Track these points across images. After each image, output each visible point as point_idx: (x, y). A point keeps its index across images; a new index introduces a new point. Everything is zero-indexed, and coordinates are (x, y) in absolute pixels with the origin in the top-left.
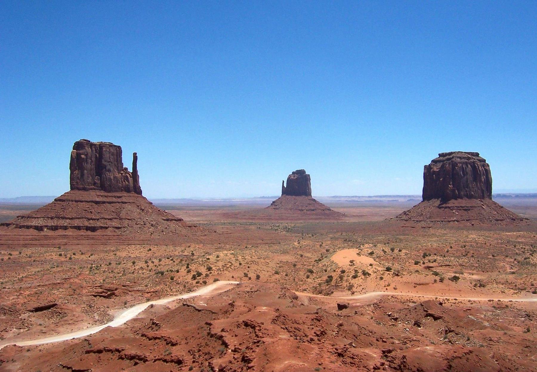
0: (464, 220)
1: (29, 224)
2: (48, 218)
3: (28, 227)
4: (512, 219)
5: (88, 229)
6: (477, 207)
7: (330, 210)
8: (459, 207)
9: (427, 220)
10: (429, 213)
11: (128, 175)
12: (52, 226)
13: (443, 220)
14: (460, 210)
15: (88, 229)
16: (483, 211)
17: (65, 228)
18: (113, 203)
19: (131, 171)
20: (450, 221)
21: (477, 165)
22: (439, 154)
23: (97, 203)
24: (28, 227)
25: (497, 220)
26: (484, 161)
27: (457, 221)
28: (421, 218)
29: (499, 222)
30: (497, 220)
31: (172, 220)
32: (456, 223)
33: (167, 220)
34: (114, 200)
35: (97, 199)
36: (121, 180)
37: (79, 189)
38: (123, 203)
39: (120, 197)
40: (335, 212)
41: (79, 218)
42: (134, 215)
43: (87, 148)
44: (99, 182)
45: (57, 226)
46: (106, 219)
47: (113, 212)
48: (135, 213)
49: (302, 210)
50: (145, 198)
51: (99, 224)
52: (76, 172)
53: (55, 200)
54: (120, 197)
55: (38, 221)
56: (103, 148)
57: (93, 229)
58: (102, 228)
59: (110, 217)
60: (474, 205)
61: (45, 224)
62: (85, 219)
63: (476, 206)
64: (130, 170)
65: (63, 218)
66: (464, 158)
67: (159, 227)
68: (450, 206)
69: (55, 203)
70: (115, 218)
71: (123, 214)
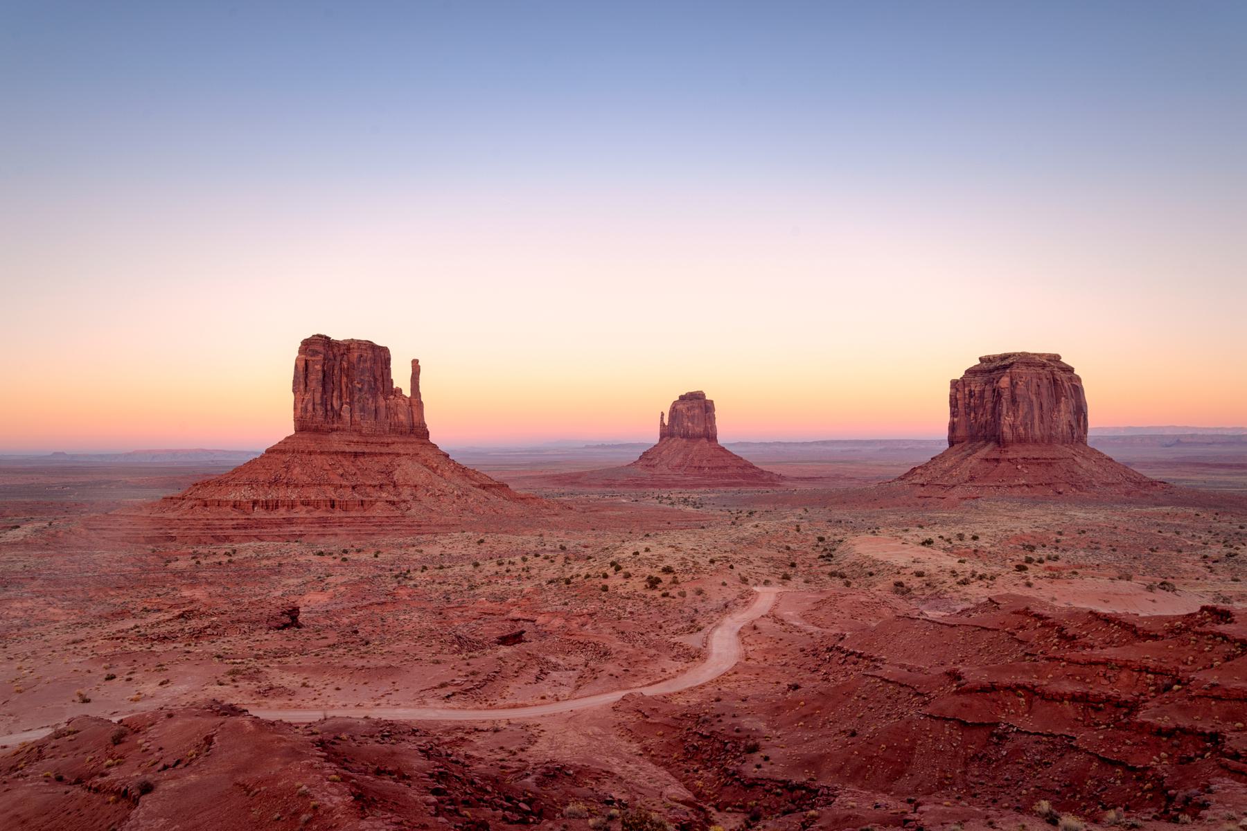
0: (1042, 484)
4: (1135, 483)
6: (1060, 459)
13: (998, 484)
16: (1076, 468)
20: (1015, 486)
25: (1107, 484)
26: (1070, 370)
27: (1027, 486)
28: (955, 481)
30: (1107, 484)
31: (491, 486)
32: (1027, 489)
33: (484, 487)
53: (269, 451)
59: (374, 483)
60: (1057, 454)
68: (1010, 457)
69: (268, 457)
70: (386, 485)
71: (398, 476)
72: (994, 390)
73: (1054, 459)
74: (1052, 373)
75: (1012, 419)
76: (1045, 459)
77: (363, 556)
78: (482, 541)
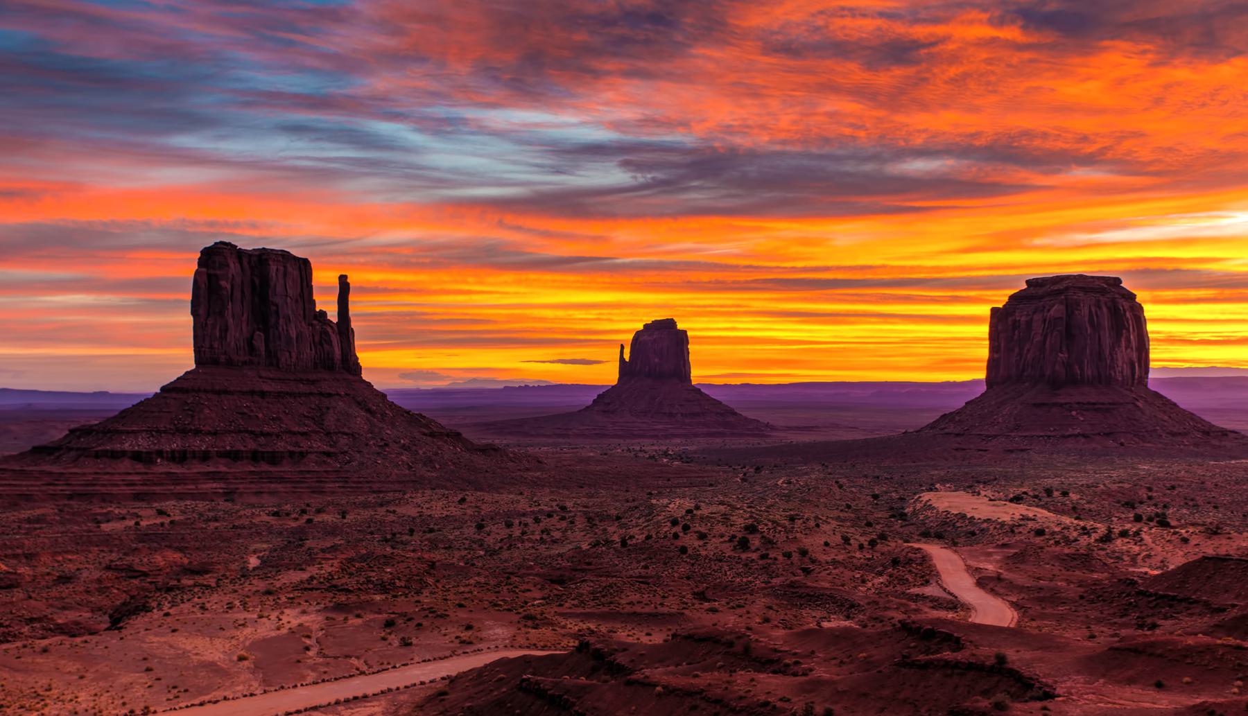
1: (118, 447)
2: (158, 431)
3: (116, 455)
5: (255, 457)
6: (1121, 404)
7: (735, 414)
8: (1084, 404)
9: (1013, 434)
10: (1012, 420)
11: (329, 330)
12: (173, 451)
13: (1049, 433)
14: (1086, 410)
15: (255, 457)
17: (205, 457)
18: (300, 395)
19: (335, 320)
21: (1123, 307)
22: (1027, 282)
23: (263, 394)
24: (116, 455)
25: (1173, 434)
27: (1084, 436)
29: (1179, 439)
30: (1173, 434)
32: (1083, 440)
33: (432, 435)
34: (303, 388)
35: (266, 388)
36: (314, 340)
37: (215, 362)
38: (321, 394)
39: (313, 382)
40: (746, 418)
41: (230, 432)
42: (356, 423)
43: (232, 265)
44: (260, 344)
45: (185, 452)
46: (294, 433)
47: (305, 416)
48: (359, 420)
49: (671, 415)
50: (369, 385)
51: (281, 446)
52: (210, 322)
54: (313, 382)
55: (136, 439)
56: (271, 263)
57: (274, 458)
58: (292, 454)
59: (301, 430)
61: (157, 447)
62: (246, 435)
63: (1122, 401)
64: (333, 316)
65: (197, 432)
66: (1092, 290)
67: (421, 452)
68: (1063, 401)
71: (330, 421)
72: (1045, 321)
73: (1113, 404)
74: (1113, 301)
75: (1066, 356)
76: (1103, 404)
77: (327, 518)
78: (463, 500)
